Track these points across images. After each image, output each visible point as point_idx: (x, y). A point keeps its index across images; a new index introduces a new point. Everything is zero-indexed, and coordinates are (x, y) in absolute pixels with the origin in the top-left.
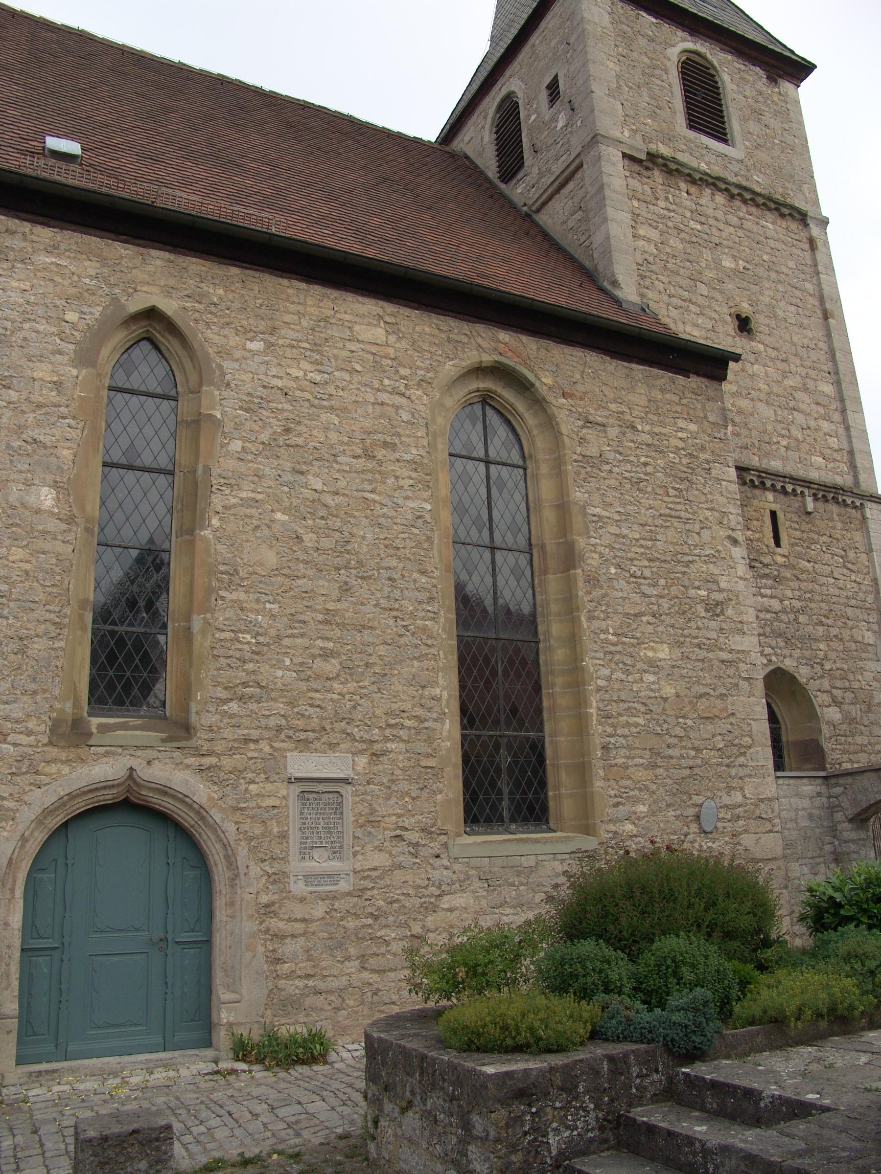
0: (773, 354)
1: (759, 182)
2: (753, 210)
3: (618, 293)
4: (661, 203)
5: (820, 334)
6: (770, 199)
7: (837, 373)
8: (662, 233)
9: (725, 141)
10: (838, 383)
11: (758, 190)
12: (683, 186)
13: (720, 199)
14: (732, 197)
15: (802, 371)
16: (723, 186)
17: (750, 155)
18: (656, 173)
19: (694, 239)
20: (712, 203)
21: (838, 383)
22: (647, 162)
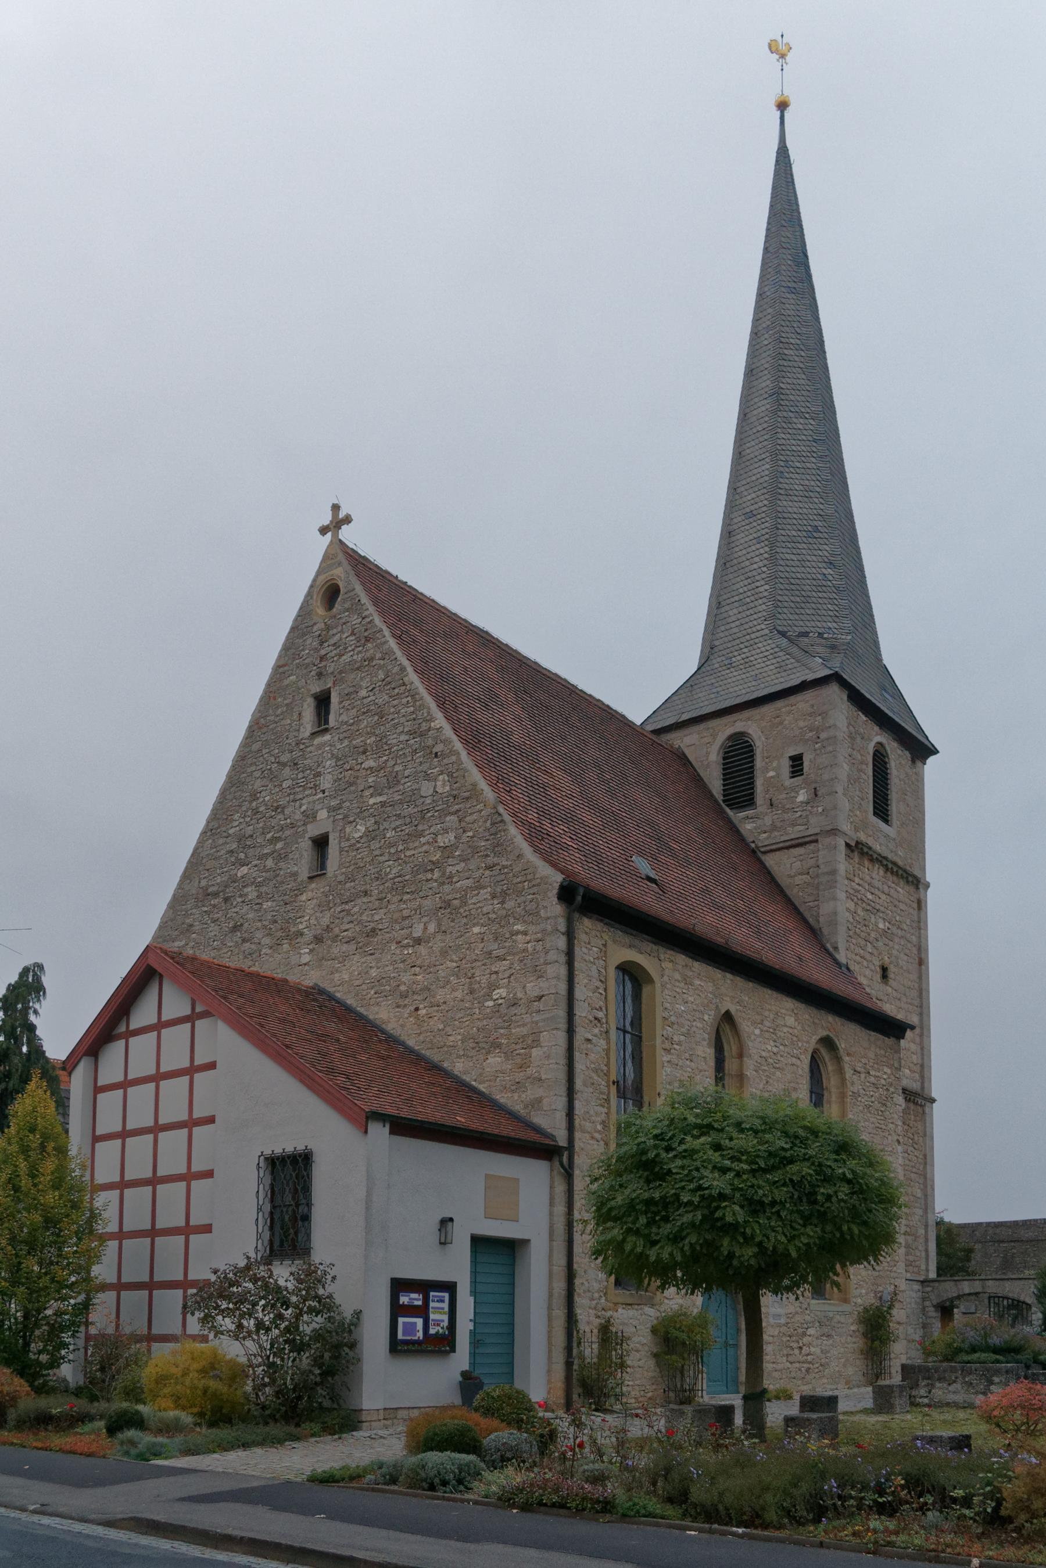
0: (895, 994)
1: (900, 856)
2: (895, 878)
3: (837, 956)
4: (857, 880)
5: (914, 976)
6: (905, 871)
7: (921, 1007)
8: (856, 904)
9: (886, 821)
10: (921, 1014)
11: (900, 863)
12: (866, 863)
13: (882, 872)
14: (887, 869)
15: (906, 1006)
16: (885, 863)
17: (899, 833)
18: (856, 853)
19: (869, 908)
20: (878, 873)
21: (921, 1014)
22: (858, 849)
